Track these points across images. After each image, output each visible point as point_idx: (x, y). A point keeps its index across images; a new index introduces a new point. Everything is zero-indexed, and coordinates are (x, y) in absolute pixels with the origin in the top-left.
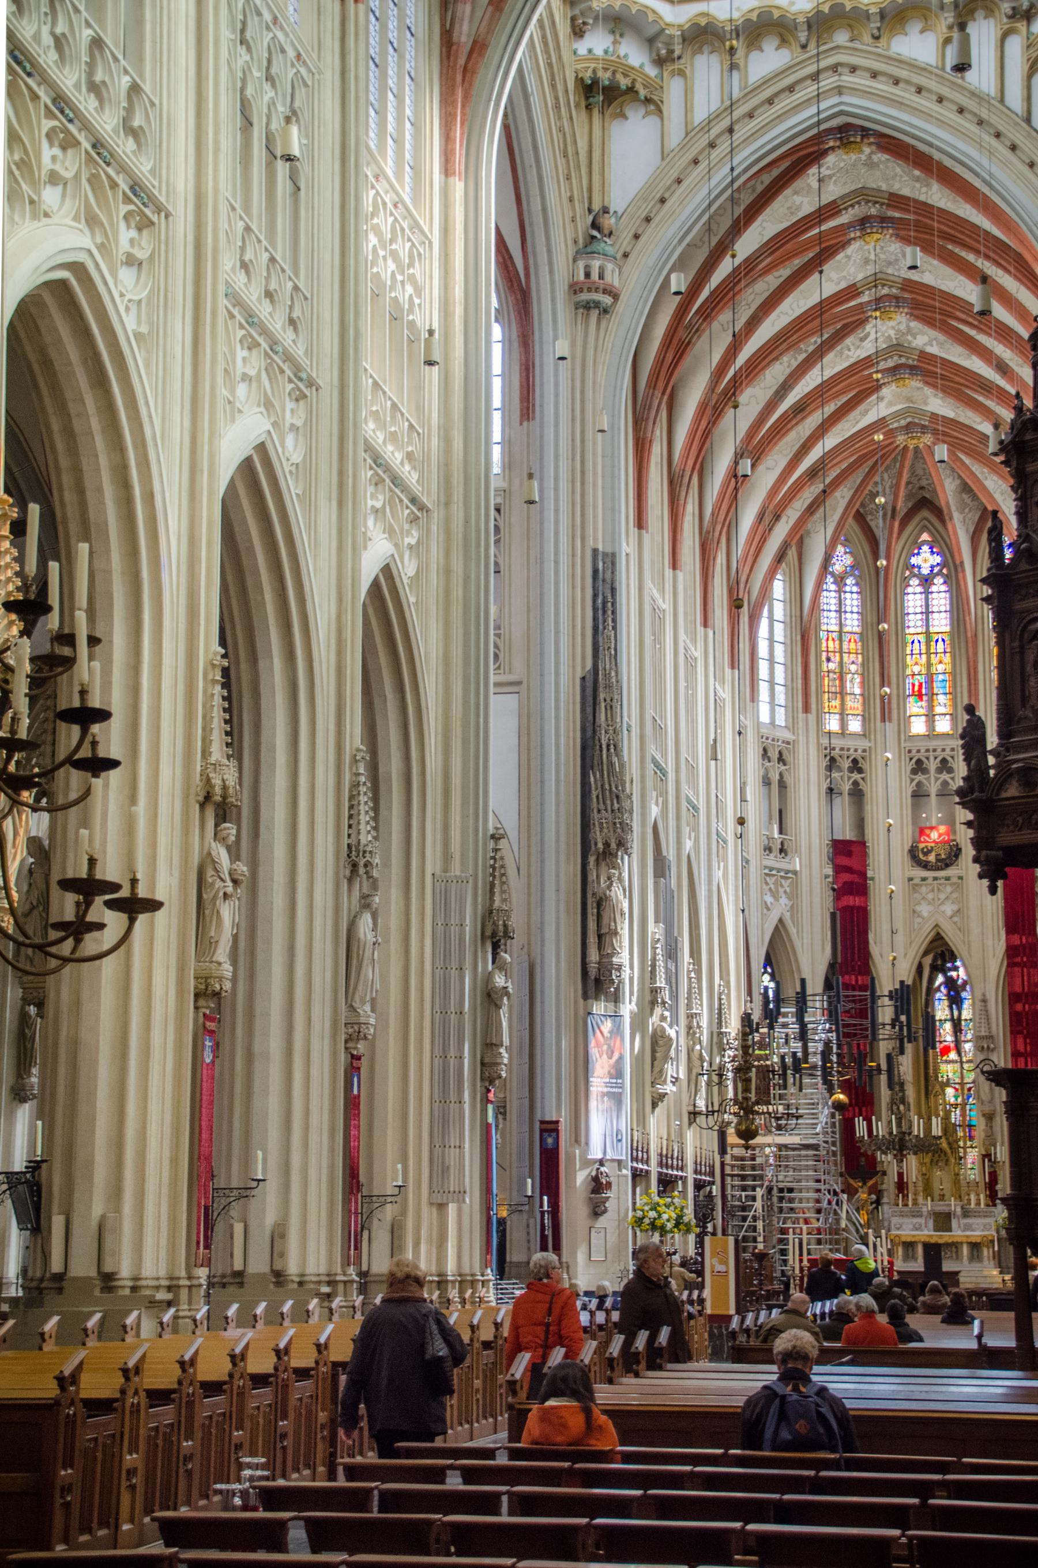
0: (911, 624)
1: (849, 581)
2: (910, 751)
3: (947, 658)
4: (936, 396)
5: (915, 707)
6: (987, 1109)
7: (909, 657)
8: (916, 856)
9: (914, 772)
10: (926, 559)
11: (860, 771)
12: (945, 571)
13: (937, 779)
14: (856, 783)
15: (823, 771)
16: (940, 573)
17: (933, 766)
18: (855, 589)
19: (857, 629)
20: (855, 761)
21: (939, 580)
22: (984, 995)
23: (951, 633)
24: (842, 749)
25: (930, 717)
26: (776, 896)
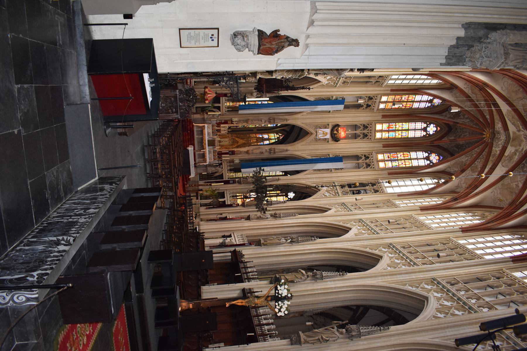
0: (412, 125)
1: (430, 104)
2: (371, 124)
3: (400, 137)
4: (516, 151)
5: (385, 126)
6: (250, 152)
7: (401, 124)
8: (336, 127)
9: (364, 125)
10: (432, 129)
11: (366, 108)
12: (427, 135)
13: (361, 133)
14: (362, 106)
15: (369, 96)
16: (427, 134)
17: (365, 131)
18: (426, 106)
19: (413, 107)
20: (370, 106)
21: (425, 133)
22: (289, 150)
23: (408, 138)
24: (375, 102)
25: (381, 131)
26: (328, 80)
